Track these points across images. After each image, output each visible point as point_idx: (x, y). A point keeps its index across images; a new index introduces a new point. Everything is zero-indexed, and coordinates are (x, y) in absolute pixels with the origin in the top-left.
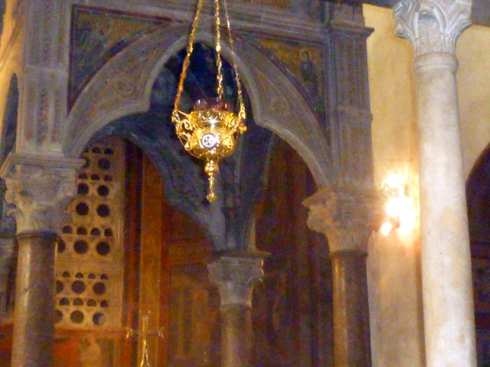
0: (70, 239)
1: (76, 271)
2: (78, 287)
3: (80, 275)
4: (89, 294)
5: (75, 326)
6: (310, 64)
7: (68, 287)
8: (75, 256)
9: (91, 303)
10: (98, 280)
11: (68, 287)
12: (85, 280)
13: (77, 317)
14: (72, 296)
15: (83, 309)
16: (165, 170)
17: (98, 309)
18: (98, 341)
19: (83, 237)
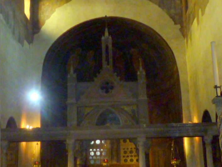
1: (130, 147)
2: (131, 152)
3: (131, 148)
5: (131, 163)
6: (134, 110)
7: (128, 152)
9: (135, 156)
11: (128, 152)
13: (132, 160)
14: (130, 154)
15: (133, 158)
17: (137, 158)
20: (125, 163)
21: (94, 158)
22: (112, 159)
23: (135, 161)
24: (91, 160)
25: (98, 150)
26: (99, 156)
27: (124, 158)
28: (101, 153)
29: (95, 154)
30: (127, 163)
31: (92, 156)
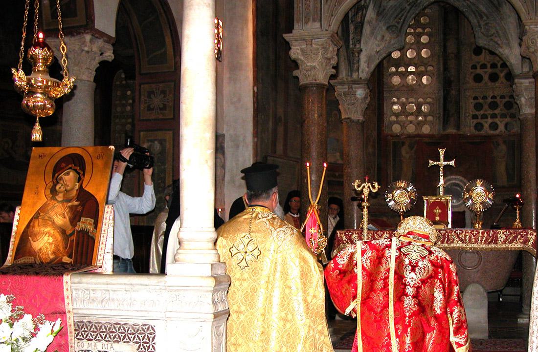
0: (486, 73)
1: (492, 95)
2: (493, 105)
3: (494, 97)
4: (501, 110)
7: (486, 107)
8: (490, 84)
9: (503, 116)
10: (507, 99)
11: (486, 107)
12: (498, 100)
13: (494, 126)
14: (490, 112)
15: (497, 120)
16: (474, 21)
17: (508, 119)
18: (504, 142)
19: (495, 70)
20: (476, 133)
21: (402, 118)
22: (445, 122)
23: (501, 127)
24: (392, 123)
25: (410, 100)
26: (412, 114)
27: (475, 121)
28: (419, 106)
29: (404, 112)
30: (482, 132)
31: (397, 115)
